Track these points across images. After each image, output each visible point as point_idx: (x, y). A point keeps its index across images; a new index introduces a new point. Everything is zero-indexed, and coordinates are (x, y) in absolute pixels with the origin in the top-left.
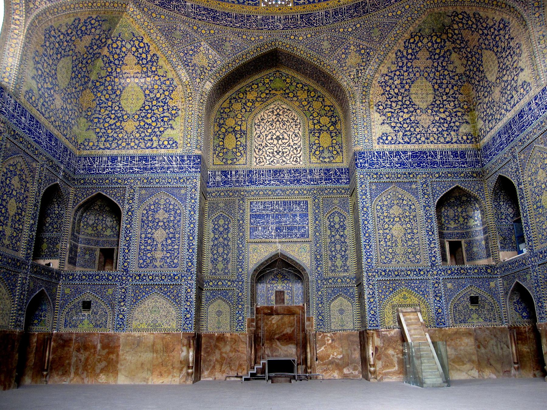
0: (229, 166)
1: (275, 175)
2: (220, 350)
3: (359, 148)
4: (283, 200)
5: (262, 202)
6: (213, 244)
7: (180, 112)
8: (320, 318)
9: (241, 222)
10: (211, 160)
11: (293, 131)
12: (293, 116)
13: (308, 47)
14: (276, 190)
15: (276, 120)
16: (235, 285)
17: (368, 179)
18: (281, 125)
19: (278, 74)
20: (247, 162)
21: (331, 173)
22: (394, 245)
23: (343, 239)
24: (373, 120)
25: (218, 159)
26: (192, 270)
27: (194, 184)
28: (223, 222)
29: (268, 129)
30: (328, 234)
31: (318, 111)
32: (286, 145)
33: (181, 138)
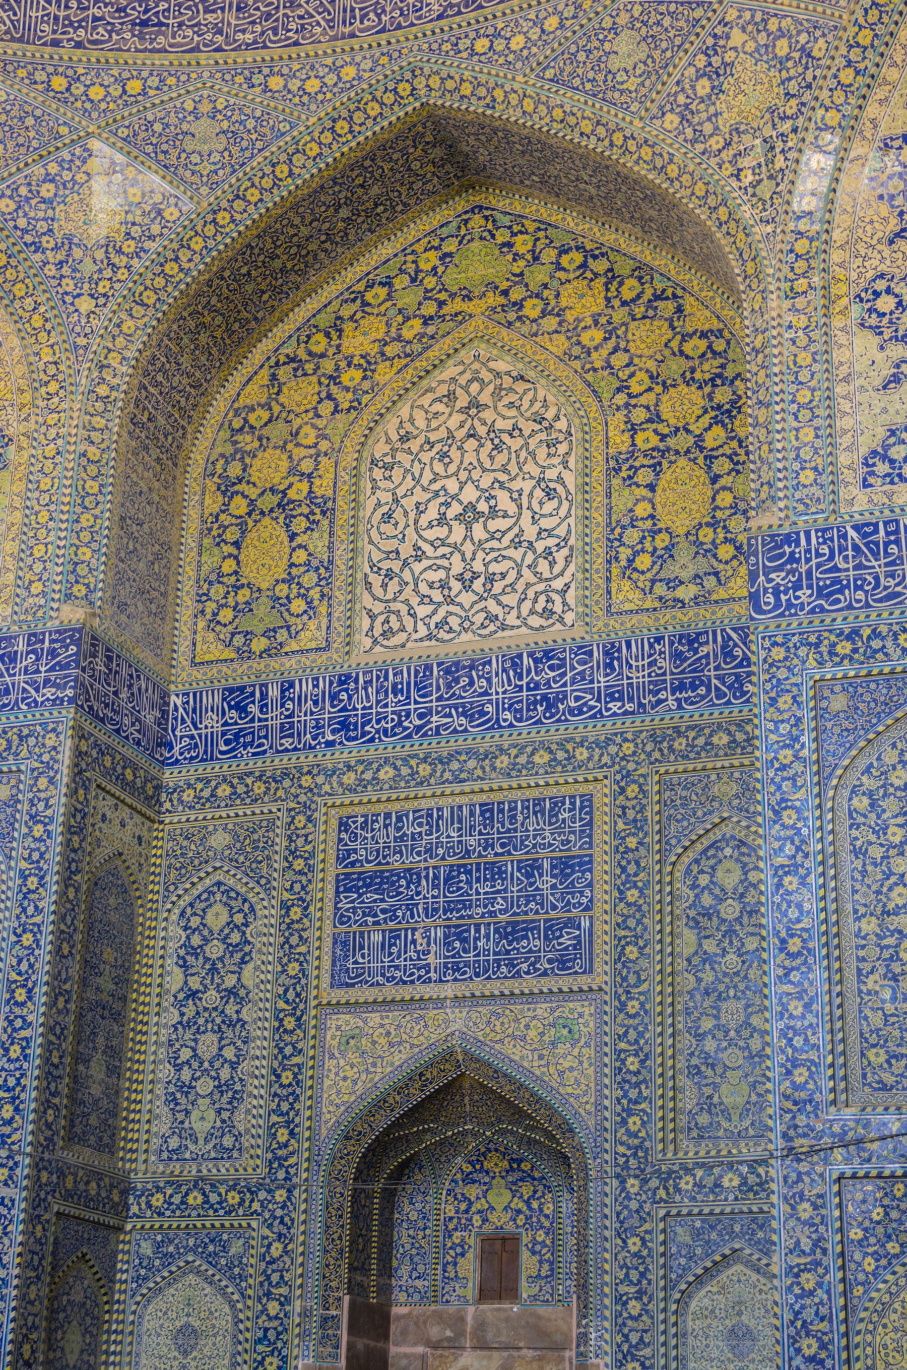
0: (258, 665)
1: (449, 687)
5: (388, 816)
6: (177, 1018)
11: (536, 471)
12: (538, 405)
13: (549, 74)
15: (461, 434)
16: (256, 1206)
17: (811, 663)
19: (477, 221)
21: (704, 650)
24: (843, 371)
25: (211, 636)
26: (15, 1137)
27: (46, 757)
28: (224, 918)
29: (425, 481)
30: (688, 951)
31: (651, 365)
32: (506, 541)
33: (10, 563)
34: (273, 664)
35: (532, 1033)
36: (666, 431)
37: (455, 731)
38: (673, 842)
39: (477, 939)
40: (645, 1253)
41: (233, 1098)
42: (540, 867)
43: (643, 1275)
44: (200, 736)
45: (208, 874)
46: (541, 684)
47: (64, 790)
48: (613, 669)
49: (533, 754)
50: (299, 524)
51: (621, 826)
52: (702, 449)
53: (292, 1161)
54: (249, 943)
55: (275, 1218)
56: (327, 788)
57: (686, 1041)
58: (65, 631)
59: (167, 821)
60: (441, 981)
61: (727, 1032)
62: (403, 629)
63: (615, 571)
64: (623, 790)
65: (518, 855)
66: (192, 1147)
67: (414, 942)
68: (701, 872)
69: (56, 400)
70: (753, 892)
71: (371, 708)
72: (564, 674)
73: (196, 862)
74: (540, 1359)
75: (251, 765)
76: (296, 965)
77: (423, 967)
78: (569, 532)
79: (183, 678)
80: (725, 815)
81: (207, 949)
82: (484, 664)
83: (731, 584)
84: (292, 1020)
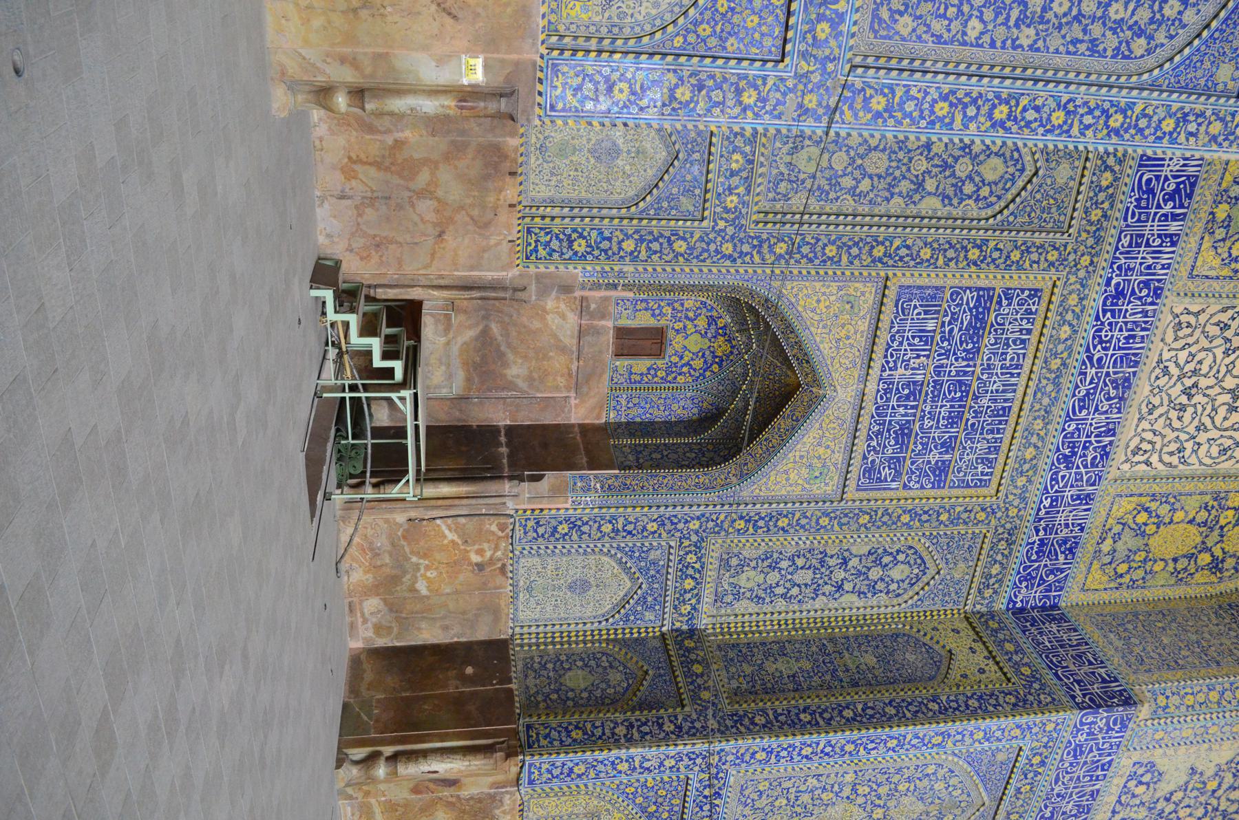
2: (447, 157)
3: (1144, 711)
4: (1015, 409)
5: (1029, 332)
8: (563, 528)
9: (974, 254)
14: (1057, 385)
16: (722, 224)
17: (1035, 744)
20: (1198, 281)
21: (1061, 558)
22: (798, 809)
28: (990, 176)
30: (854, 550)
35: (821, 450)
37: (1077, 387)
39: (906, 407)
40: (645, 534)
41: (823, 191)
42: (947, 452)
43: (630, 533)
46: (1085, 451)
49: (1035, 446)
51: (958, 509)
52: (1200, 552)
53: (757, 258)
55: (708, 244)
56: (1073, 279)
57: (791, 551)
61: (791, 574)
62: (1176, 340)
63: (1143, 499)
64: (983, 510)
66: (785, 150)
67: (918, 357)
68: (907, 555)
71: (1125, 317)
72: (1085, 467)
74: (570, 375)
75: (1120, 206)
77: (896, 365)
78: (1189, 464)
81: (967, 160)
82: (1119, 409)
84: (881, 254)
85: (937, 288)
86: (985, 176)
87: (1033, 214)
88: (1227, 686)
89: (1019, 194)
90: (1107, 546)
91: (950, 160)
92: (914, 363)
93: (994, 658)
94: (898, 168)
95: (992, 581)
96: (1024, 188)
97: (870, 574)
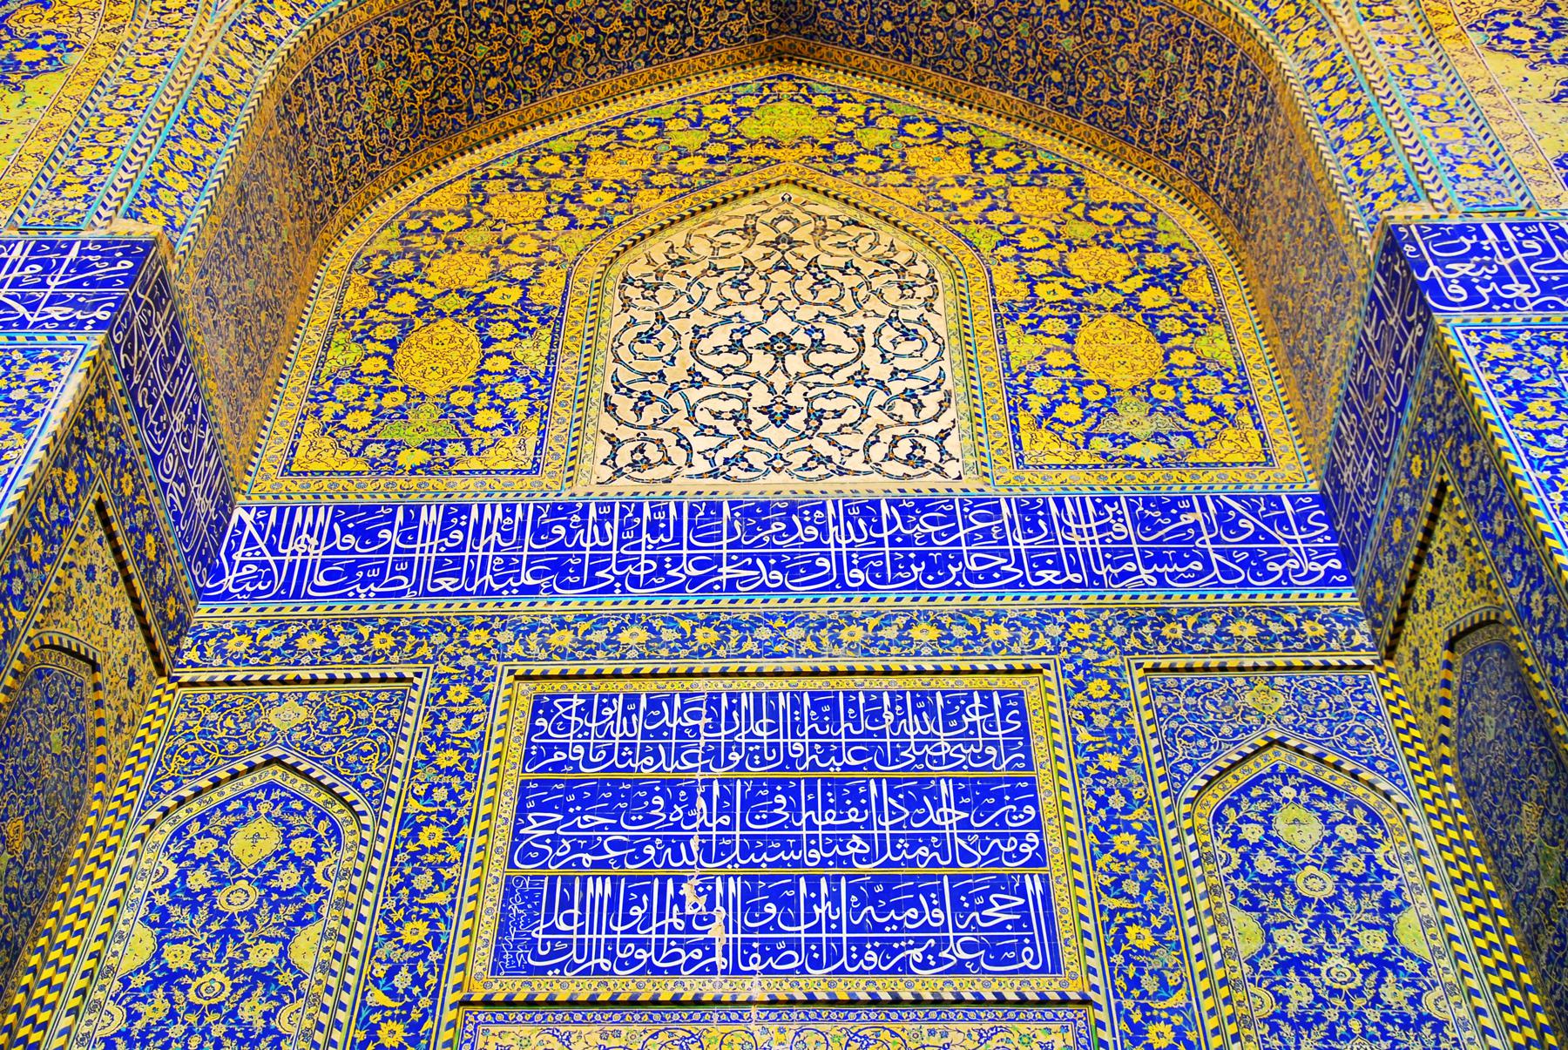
1: (751, 532)
4: (818, 684)
5: (632, 698)
7: (75, 58)
9: (431, 836)
10: (274, 451)
12: (879, 250)
14: (755, 622)
18: (802, 287)
19: (785, 87)
21: (1190, 518)
23: (1394, 994)
24: (1481, 85)
25: (327, 442)
28: (272, 839)
31: (1044, 224)
32: (841, 376)
34: (433, 481)
36: (1080, 286)
37: (763, 588)
38: (1187, 768)
44: (280, 564)
45: (252, 768)
47: (45, 440)
48: (1039, 531)
49: (908, 626)
50: (501, 330)
51: (1084, 736)
52: (1138, 308)
54: (318, 888)
56: (517, 649)
58: (117, 243)
59: (185, 678)
60: (737, 971)
62: (668, 461)
63: (1024, 419)
64: (1080, 687)
65: (888, 771)
67: (679, 900)
69: (177, 16)
70: (1353, 858)
71: (610, 547)
72: (955, 530)
73: (231, 747)
75: (372, 608)
76: (423, 927)
78: (942, 375)
79: (261, 487)
80: (1276, 735)
81: (221, 897)
82: (813, 510)
83: (1217, 446)
84: (399, 1028)
85: (509, 892)
86: (267, 852)
87: (366, 748)
88: (1328, 124)
89: (317, 781)
90: (1150, 451)
91: (215, 927)
92: (694, 902)
93: (1423, 546)
94: (208, 1029)
95: (1276, 628)
96: (306, 775)
97: (1318, 896)
